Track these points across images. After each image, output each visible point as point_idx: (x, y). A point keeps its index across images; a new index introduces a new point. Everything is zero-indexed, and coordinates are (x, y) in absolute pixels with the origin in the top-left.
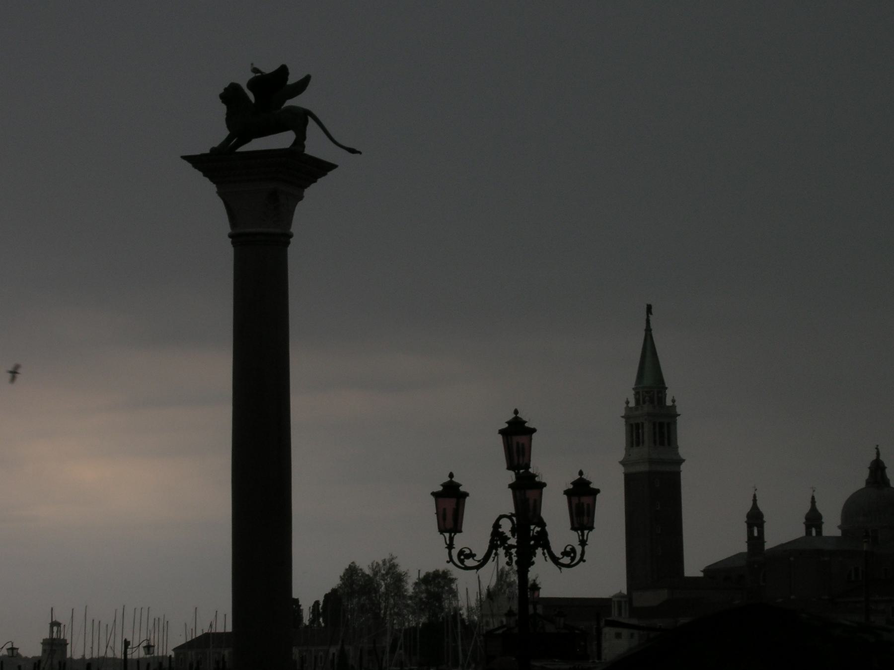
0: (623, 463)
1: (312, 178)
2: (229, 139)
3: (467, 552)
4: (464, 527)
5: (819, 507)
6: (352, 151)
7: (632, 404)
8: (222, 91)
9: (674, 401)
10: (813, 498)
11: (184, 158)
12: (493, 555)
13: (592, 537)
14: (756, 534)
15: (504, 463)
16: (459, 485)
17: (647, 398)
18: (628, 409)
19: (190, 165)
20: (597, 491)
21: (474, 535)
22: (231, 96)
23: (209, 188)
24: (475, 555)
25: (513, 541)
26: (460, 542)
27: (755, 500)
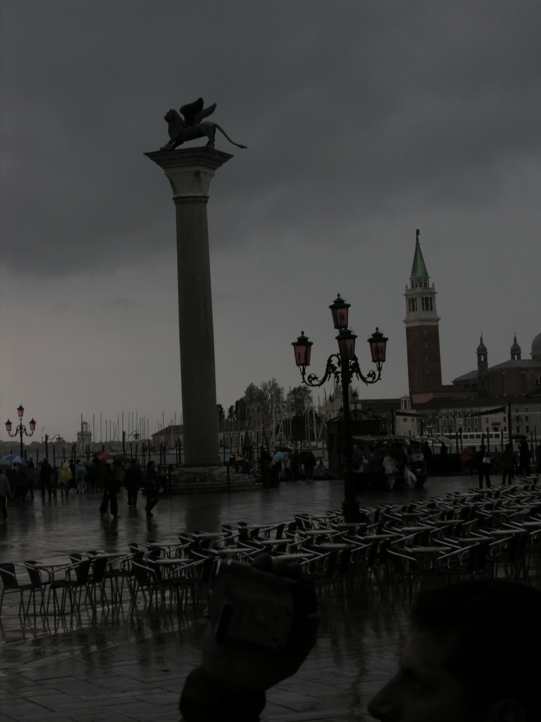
0: (405, 322)
1: (220, 163)
2: (170, 142)
3: (313, 376)
5: (518, 343)
6: (242, 147)
7: (410, 287)
8: (165, 114)
9: (433, 285)
10: (515, 338)
11: (145, 154)
12: (328, 378)
13: (385, 365)
14: (482, 359)
15: (332, 325)
16: (307, 339)
17: (418, 284)
18: (407, 290)
19: (148, 159)
20: (386, 340)
21: (317, 366)
22: (171, 117)
23: (159, 171)
24: (318, 378)
25: (339, 369)
26: (309, 370)
27: (481, 340)
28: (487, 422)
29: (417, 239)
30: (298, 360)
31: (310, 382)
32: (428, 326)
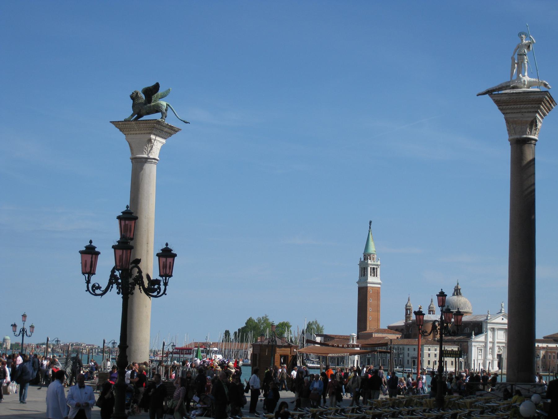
2: (133, 115)
3: (97, 285)
4: (97, 271)
7: (363, 260)
11: (112, 122)
13: (171, 280)
19: (113, 126)
20: (175, 255)
22: (134, 97)
23: (121, 136)
24: (101, 288)
26: (94, 280)
28: (408, 356)
29: (370, 227)
30: (84, 268)
31: (94, 291)
32: (373, 287)
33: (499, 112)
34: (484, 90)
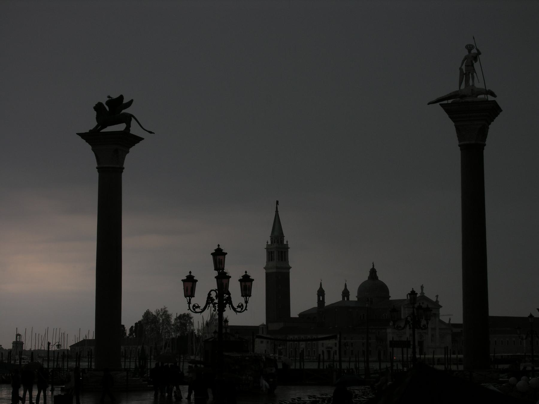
2: (97, 126)
3: (197, 305)
4: (196, 294)
5: (348, 288)
6: (151, 132)
7: (270, 243)
9: (287, 242)
10: (346, 284)
11: (78, 134)
13: (250, 299)
15: (213, 268)
18: (268, 245)
21: (200, 298)
22: (99, 108)
23: (88, 147)
25: (216, 301)
26: (194, 301)
27: (321, 285)
28: (323, 346)
33: (450, 120)
34: (434, 99)
